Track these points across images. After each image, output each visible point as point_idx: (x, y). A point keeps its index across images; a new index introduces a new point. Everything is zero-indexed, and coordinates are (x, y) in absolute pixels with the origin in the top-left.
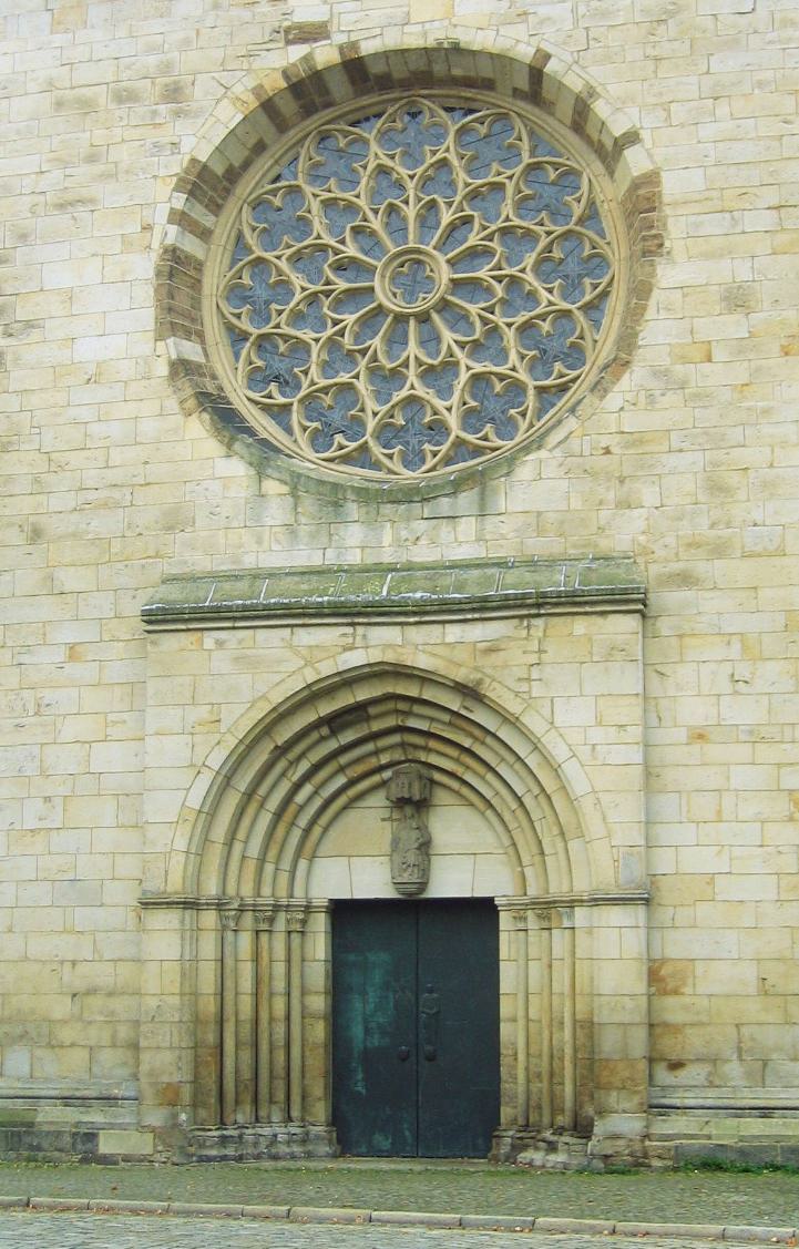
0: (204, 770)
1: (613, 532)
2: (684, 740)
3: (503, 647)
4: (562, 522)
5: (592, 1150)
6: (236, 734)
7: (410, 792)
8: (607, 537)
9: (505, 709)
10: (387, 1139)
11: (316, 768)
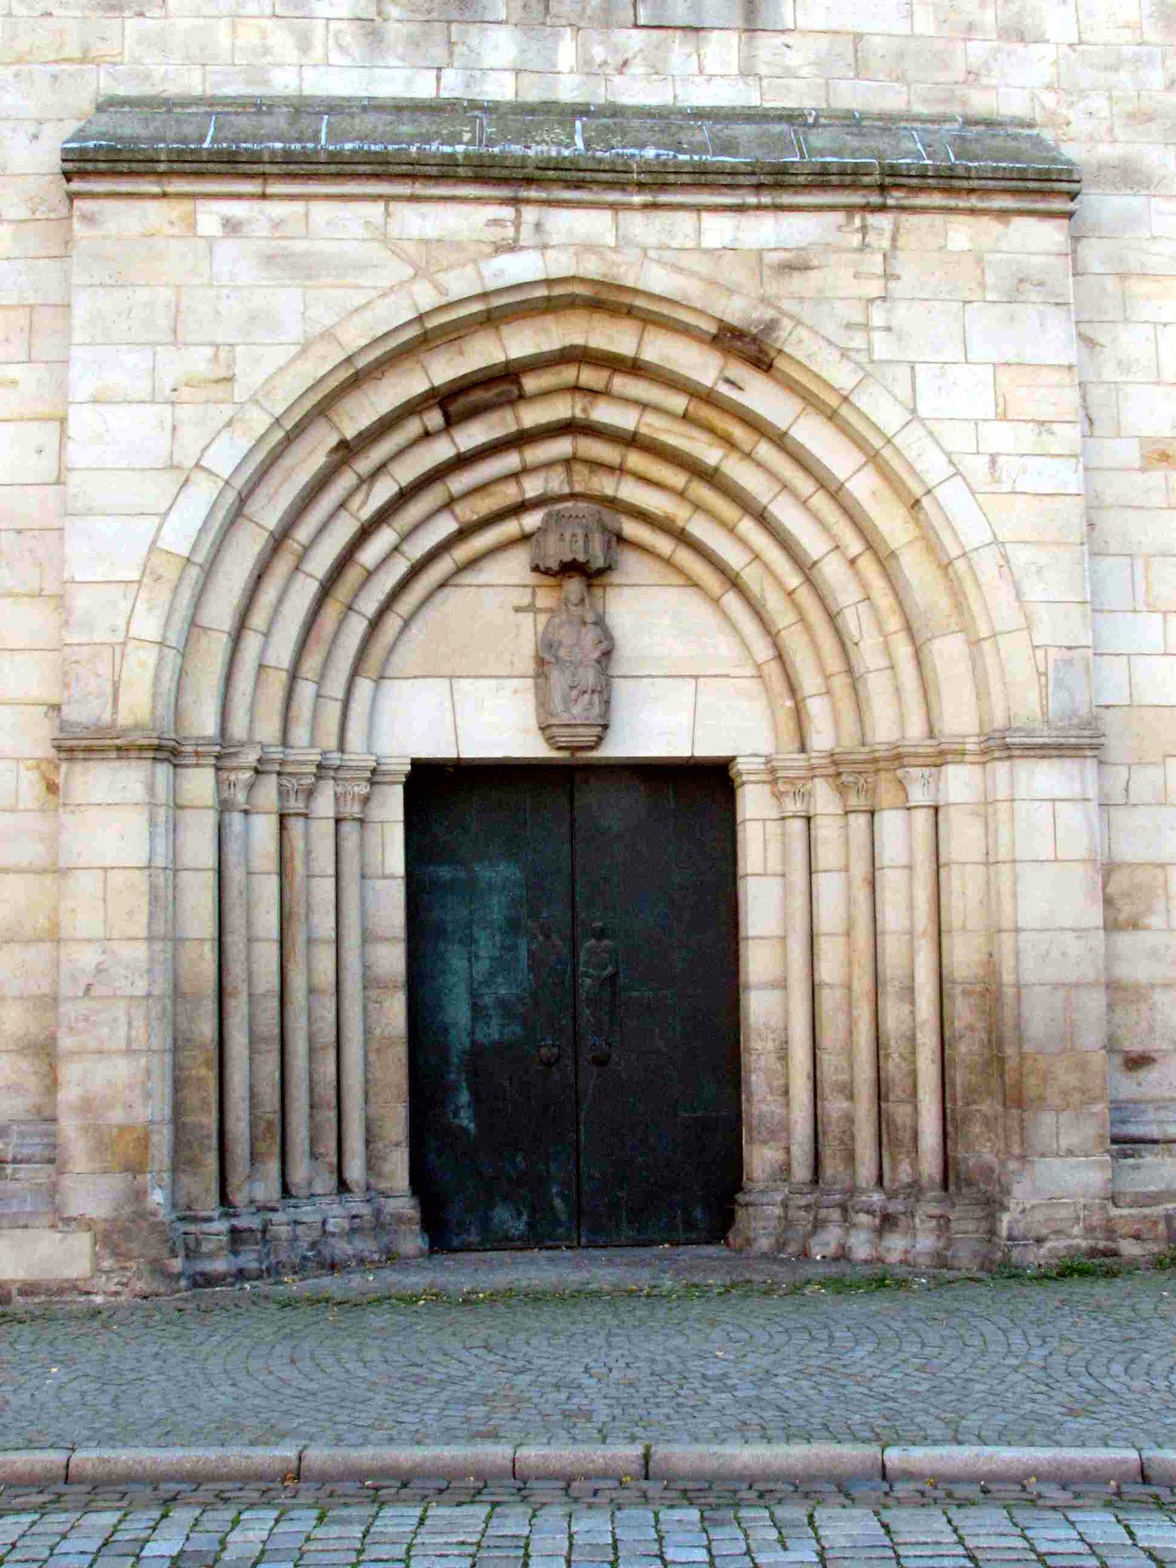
0: (199, 477)
1: (994, 82)
2: (1137, 464)
3: (816, 263)
4: (901, 55)
5: (1010, 1229)
6: (268, 405)
7: (586, 550)
8: (986, 88)
9: (817, 376)
10: (520, 1214)
11: (405, 496)
